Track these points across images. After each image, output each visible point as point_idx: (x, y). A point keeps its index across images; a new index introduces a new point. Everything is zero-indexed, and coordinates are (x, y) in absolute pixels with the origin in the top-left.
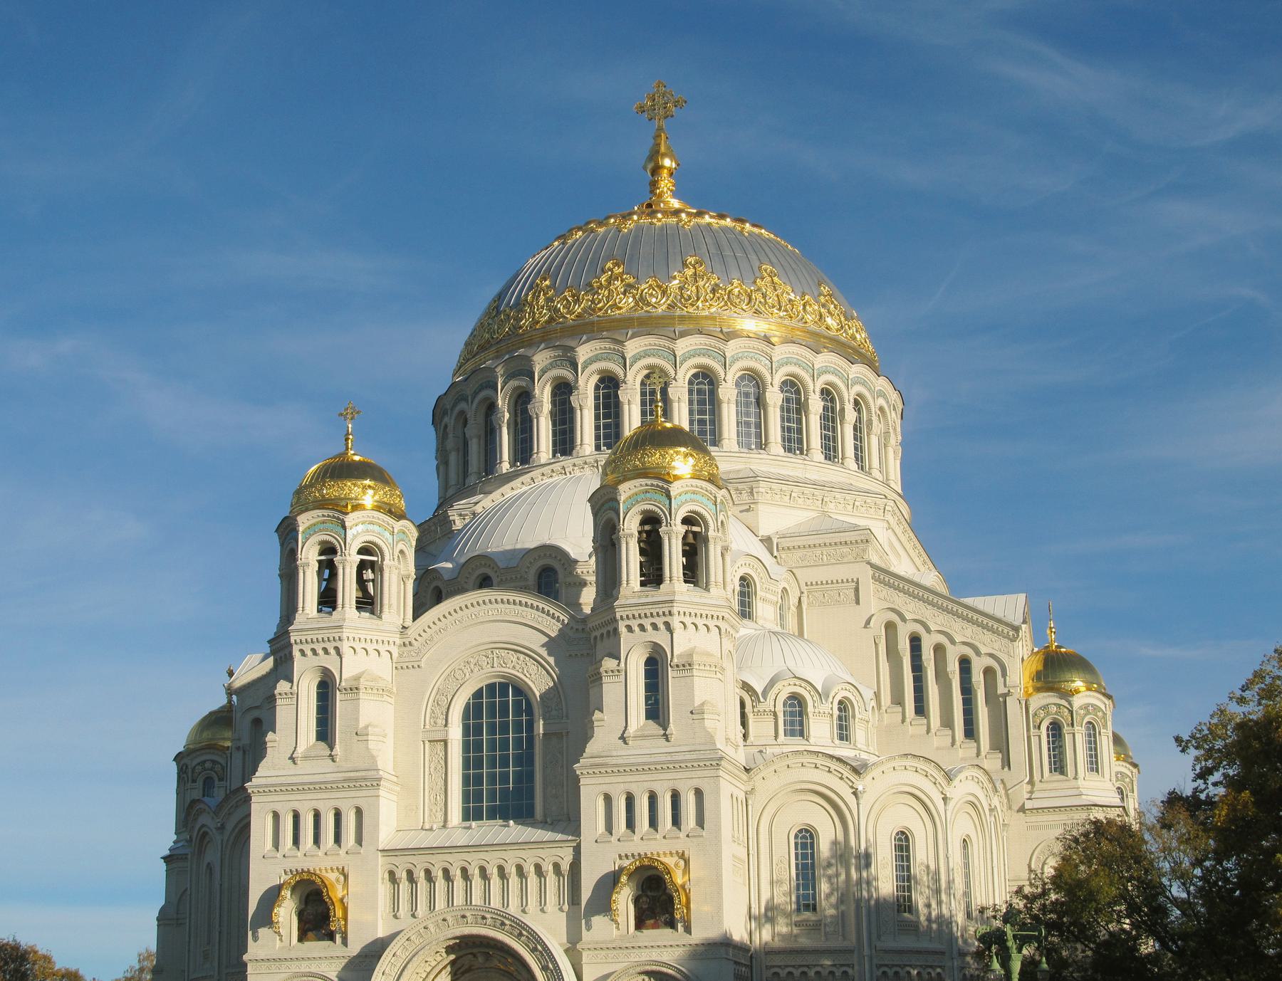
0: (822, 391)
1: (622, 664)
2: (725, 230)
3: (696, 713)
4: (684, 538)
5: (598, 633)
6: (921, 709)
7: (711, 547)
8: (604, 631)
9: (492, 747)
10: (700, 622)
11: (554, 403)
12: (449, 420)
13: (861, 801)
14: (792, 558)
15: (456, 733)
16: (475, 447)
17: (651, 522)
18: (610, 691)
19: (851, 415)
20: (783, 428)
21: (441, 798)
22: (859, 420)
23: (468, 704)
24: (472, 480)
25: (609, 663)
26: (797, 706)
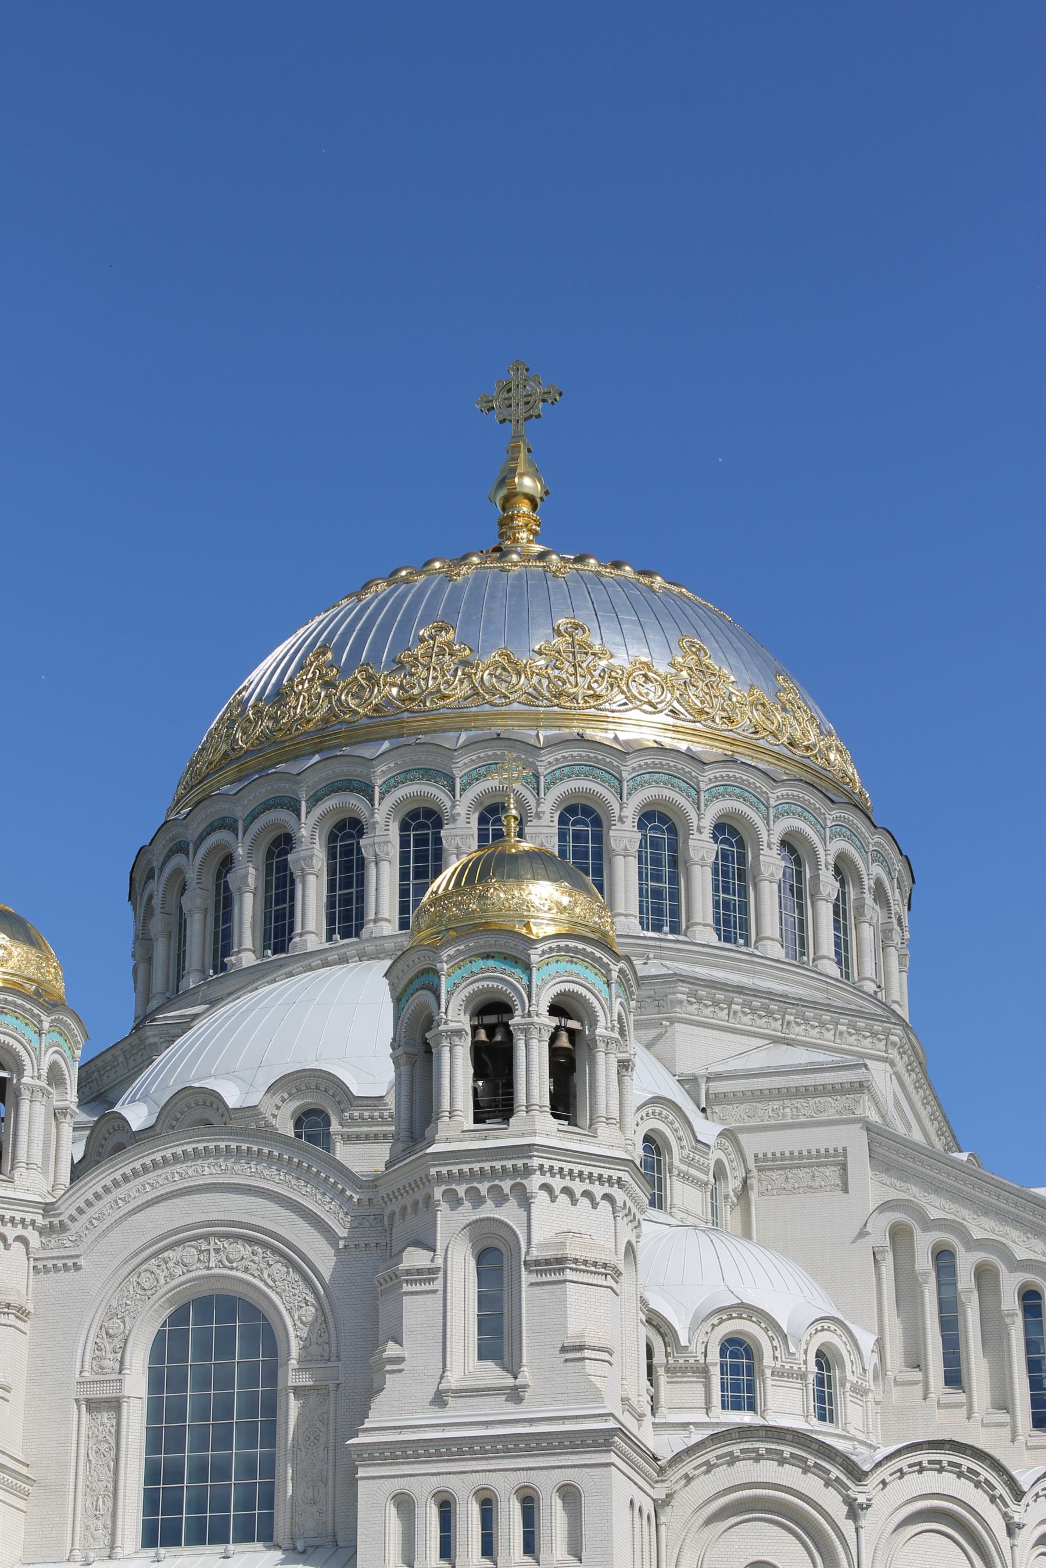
0: (783, 843)
1: (439, 1261)
2: (623, 584)
3: (574, 1351)
4: (554, 1038)
5: (394, 1207)
6: (954, 1378)
7: (601, 1057)
8: (407, 1201)
9: (202, 1413)
10: (578, 1187)
11: (331, 854)
12: (157, 887)
13: (862, 1522)
14: (736, 1115)
15: (136, 1384)
16: (198, 929)
17: (493, 1013)
18: (416, 1310)
19: (829, 885)
20: (716, 904)
21: (105, 1506)
22: (843, 895)
23: (160, 1335)
24: (191, 982)
25: (415, 1258)
26: (739, 1354)
